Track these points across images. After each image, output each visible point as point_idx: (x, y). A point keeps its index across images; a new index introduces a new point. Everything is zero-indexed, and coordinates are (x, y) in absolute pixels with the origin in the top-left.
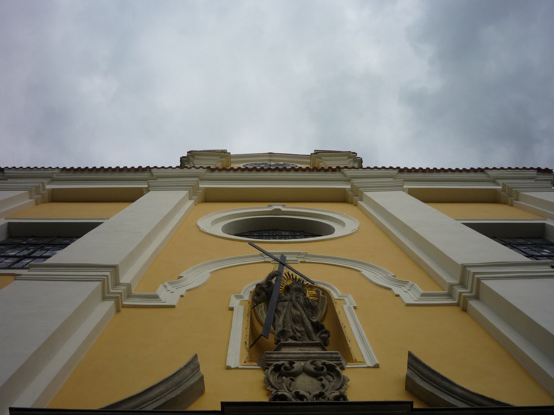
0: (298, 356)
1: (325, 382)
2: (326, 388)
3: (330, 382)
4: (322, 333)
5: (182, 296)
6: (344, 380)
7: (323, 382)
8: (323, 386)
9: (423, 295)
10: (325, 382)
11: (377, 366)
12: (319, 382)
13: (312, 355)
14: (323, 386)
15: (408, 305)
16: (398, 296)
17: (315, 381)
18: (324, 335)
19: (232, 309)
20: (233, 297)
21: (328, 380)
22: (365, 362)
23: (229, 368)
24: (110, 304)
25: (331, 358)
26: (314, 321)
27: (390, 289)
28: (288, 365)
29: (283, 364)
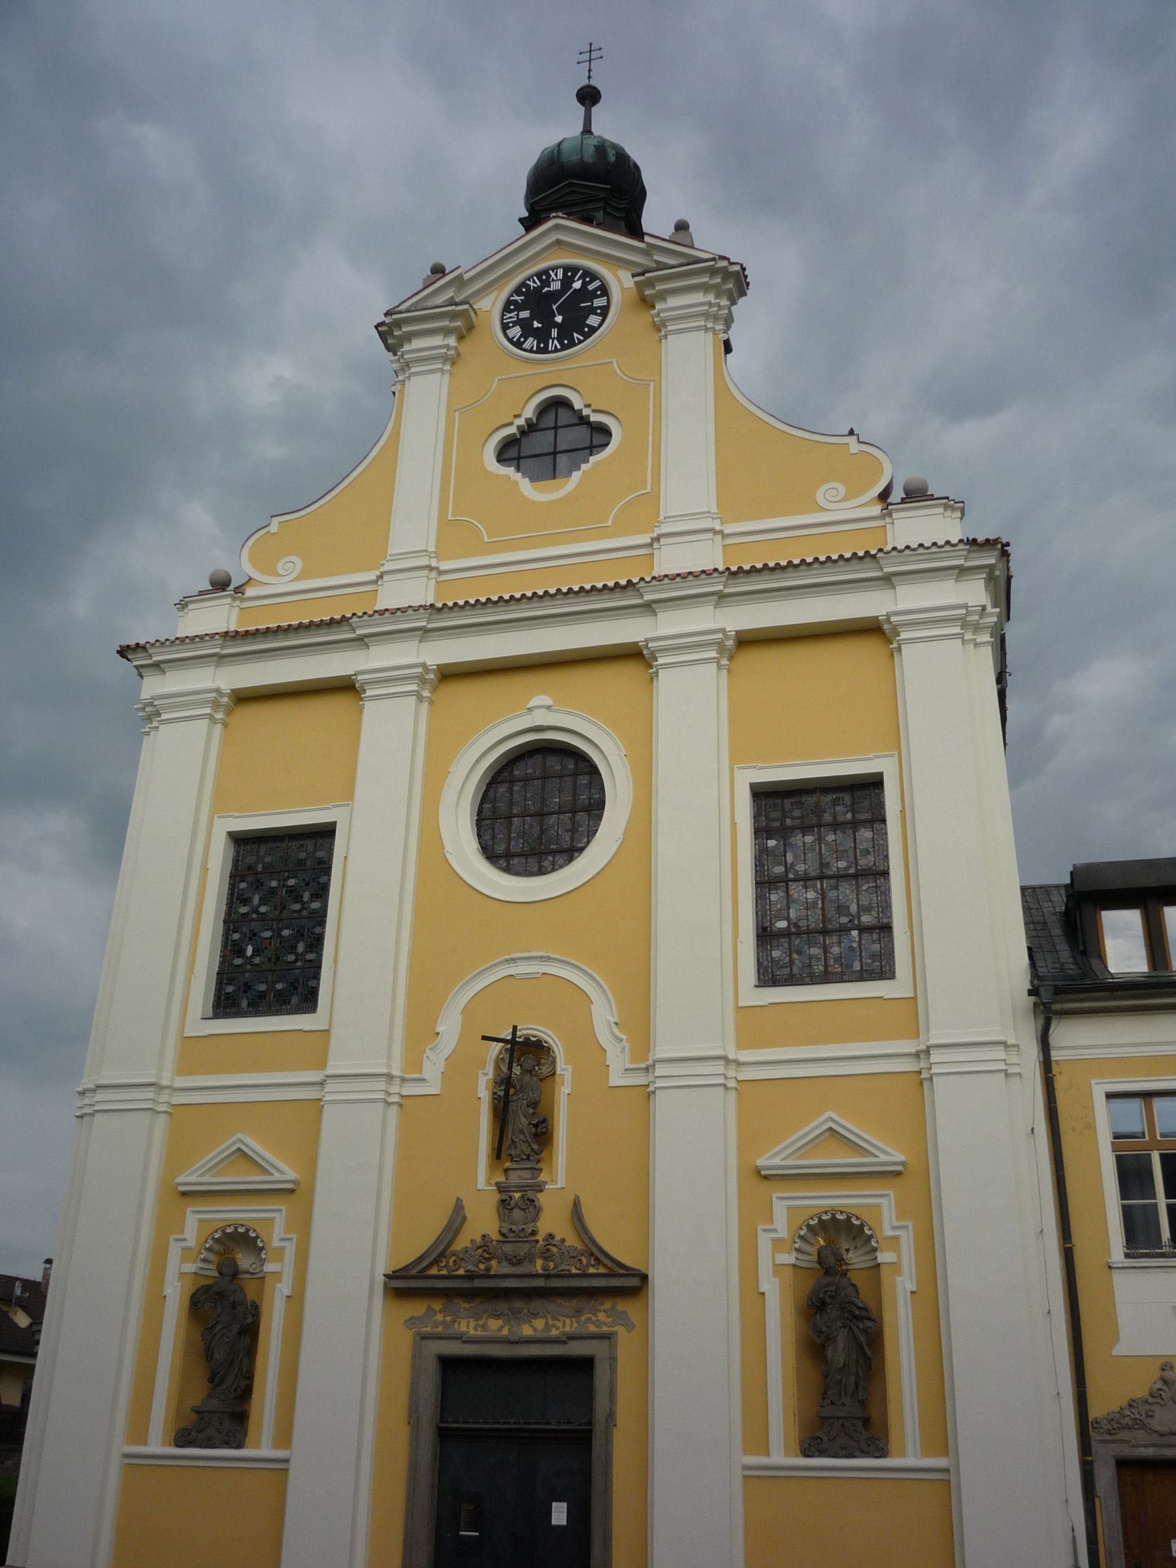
24: (395, 1108)
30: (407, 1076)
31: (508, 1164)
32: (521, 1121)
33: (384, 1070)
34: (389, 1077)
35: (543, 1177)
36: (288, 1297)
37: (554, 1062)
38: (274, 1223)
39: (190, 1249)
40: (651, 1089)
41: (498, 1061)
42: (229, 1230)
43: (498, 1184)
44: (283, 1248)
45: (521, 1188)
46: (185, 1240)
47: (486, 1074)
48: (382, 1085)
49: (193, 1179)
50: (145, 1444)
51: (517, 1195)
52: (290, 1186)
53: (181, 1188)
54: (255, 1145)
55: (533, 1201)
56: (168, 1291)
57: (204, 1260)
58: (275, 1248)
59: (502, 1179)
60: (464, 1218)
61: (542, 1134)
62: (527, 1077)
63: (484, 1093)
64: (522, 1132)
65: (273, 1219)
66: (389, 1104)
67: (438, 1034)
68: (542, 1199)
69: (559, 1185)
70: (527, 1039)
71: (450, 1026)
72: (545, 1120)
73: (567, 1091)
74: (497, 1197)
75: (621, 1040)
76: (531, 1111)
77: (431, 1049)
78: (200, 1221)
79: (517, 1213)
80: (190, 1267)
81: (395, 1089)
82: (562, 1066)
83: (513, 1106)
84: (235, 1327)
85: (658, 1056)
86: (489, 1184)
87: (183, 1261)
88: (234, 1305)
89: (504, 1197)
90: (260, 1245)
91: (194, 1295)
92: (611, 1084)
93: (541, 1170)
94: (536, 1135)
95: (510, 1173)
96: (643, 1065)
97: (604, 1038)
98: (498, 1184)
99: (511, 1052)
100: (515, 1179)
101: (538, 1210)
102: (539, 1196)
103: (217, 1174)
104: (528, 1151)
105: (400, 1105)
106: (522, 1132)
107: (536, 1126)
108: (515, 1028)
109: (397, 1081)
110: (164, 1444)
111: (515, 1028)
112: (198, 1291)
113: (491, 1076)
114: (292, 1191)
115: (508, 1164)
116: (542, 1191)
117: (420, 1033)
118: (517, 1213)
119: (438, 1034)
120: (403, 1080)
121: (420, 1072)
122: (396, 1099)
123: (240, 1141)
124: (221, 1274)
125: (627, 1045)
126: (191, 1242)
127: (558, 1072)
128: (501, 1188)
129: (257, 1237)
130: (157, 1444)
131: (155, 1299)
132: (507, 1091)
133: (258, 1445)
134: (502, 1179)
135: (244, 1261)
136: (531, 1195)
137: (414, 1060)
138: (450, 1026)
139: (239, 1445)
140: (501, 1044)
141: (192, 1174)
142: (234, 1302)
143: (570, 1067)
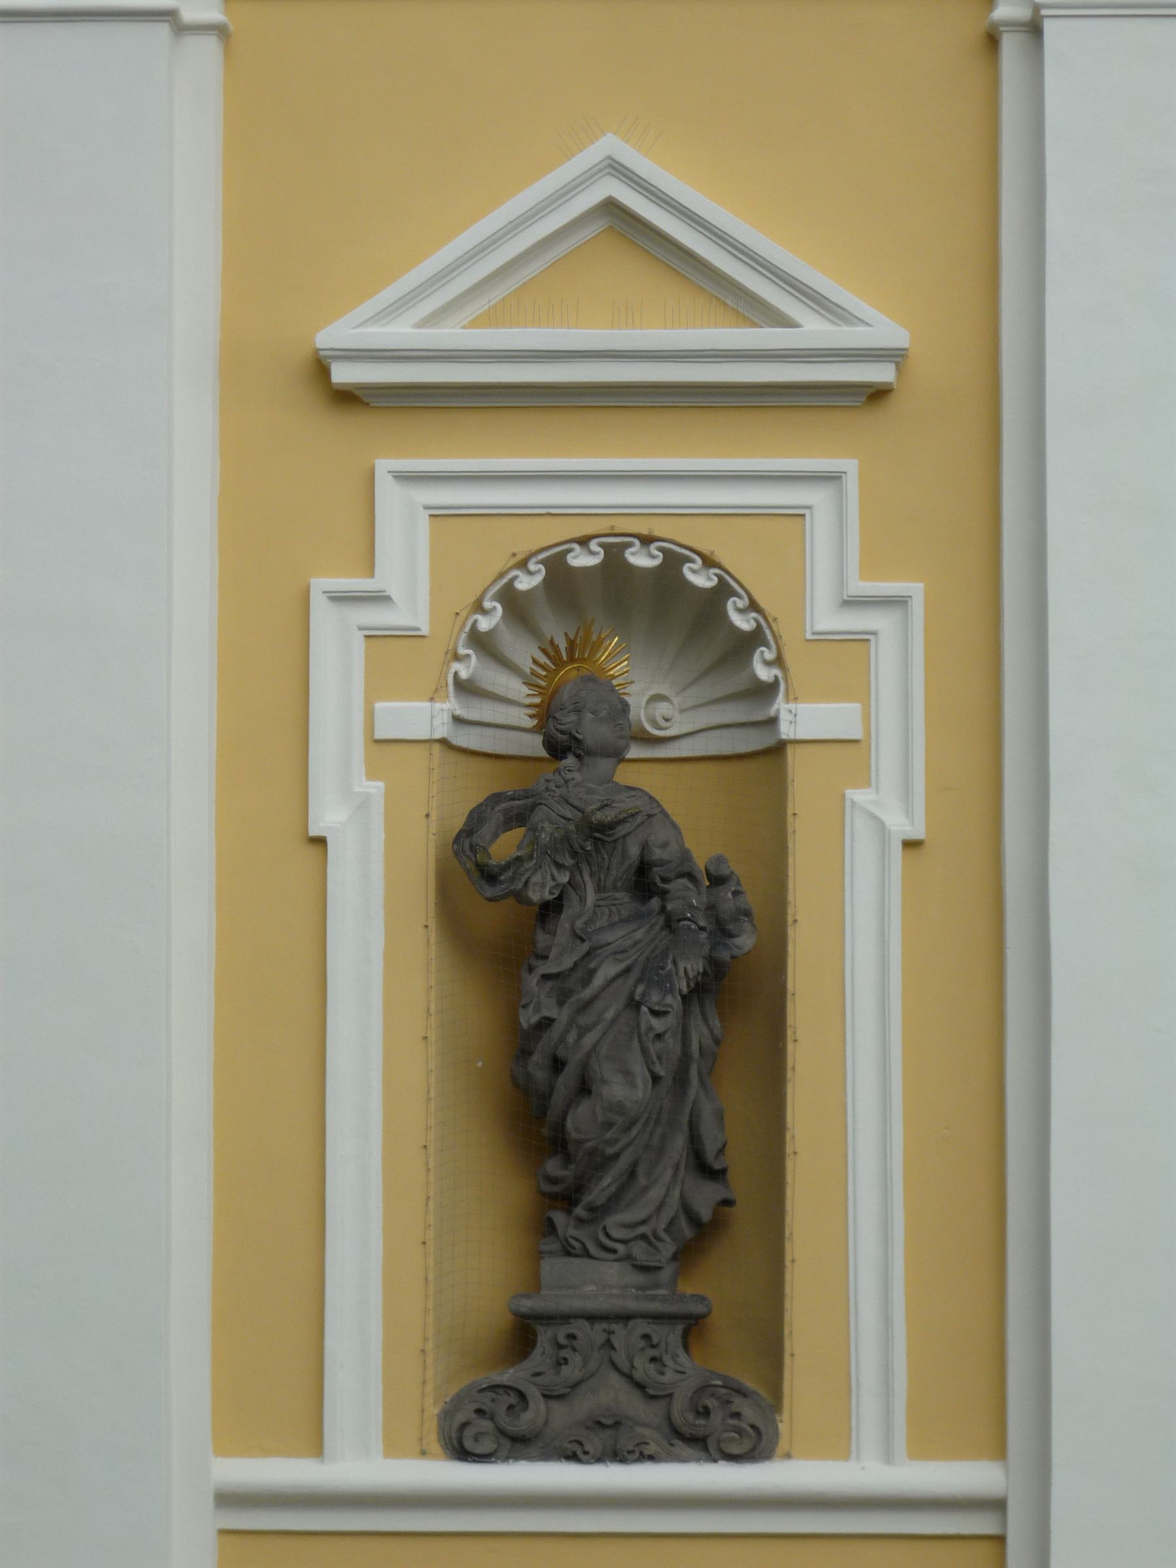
36: (910, 845)
38: (818, 545)
39: (410, 636)
42: (641, 559)
44: (862, 640)
46: (380, 599)
49: (401, 332)
50: (316, 1447)
52: (882, 374)
53: (342, 374)
54: (689, 190)
56: (329, 816)
57: (464, 688)
58: (825, 639)
65: (797, 516)
78: (439, 515)
80: (424, 716)
84: (692, 966)
87: (379, 683)
88: (644, 881)
90: (743, 623)
91: (469, 831)
103: (490, 319)
110: (393, 1449)
112: (476, 819)
114: (877, 394)
123: (615, 168)
124: (557, 749)
126: (411, 609)
129: (723, 591)
130: (369, 1449)
131: (274, 858)
133: (838, 1442)
135: (651, 689)
139: (756, 1446)
141: (375, 319)
142: (643, 868)
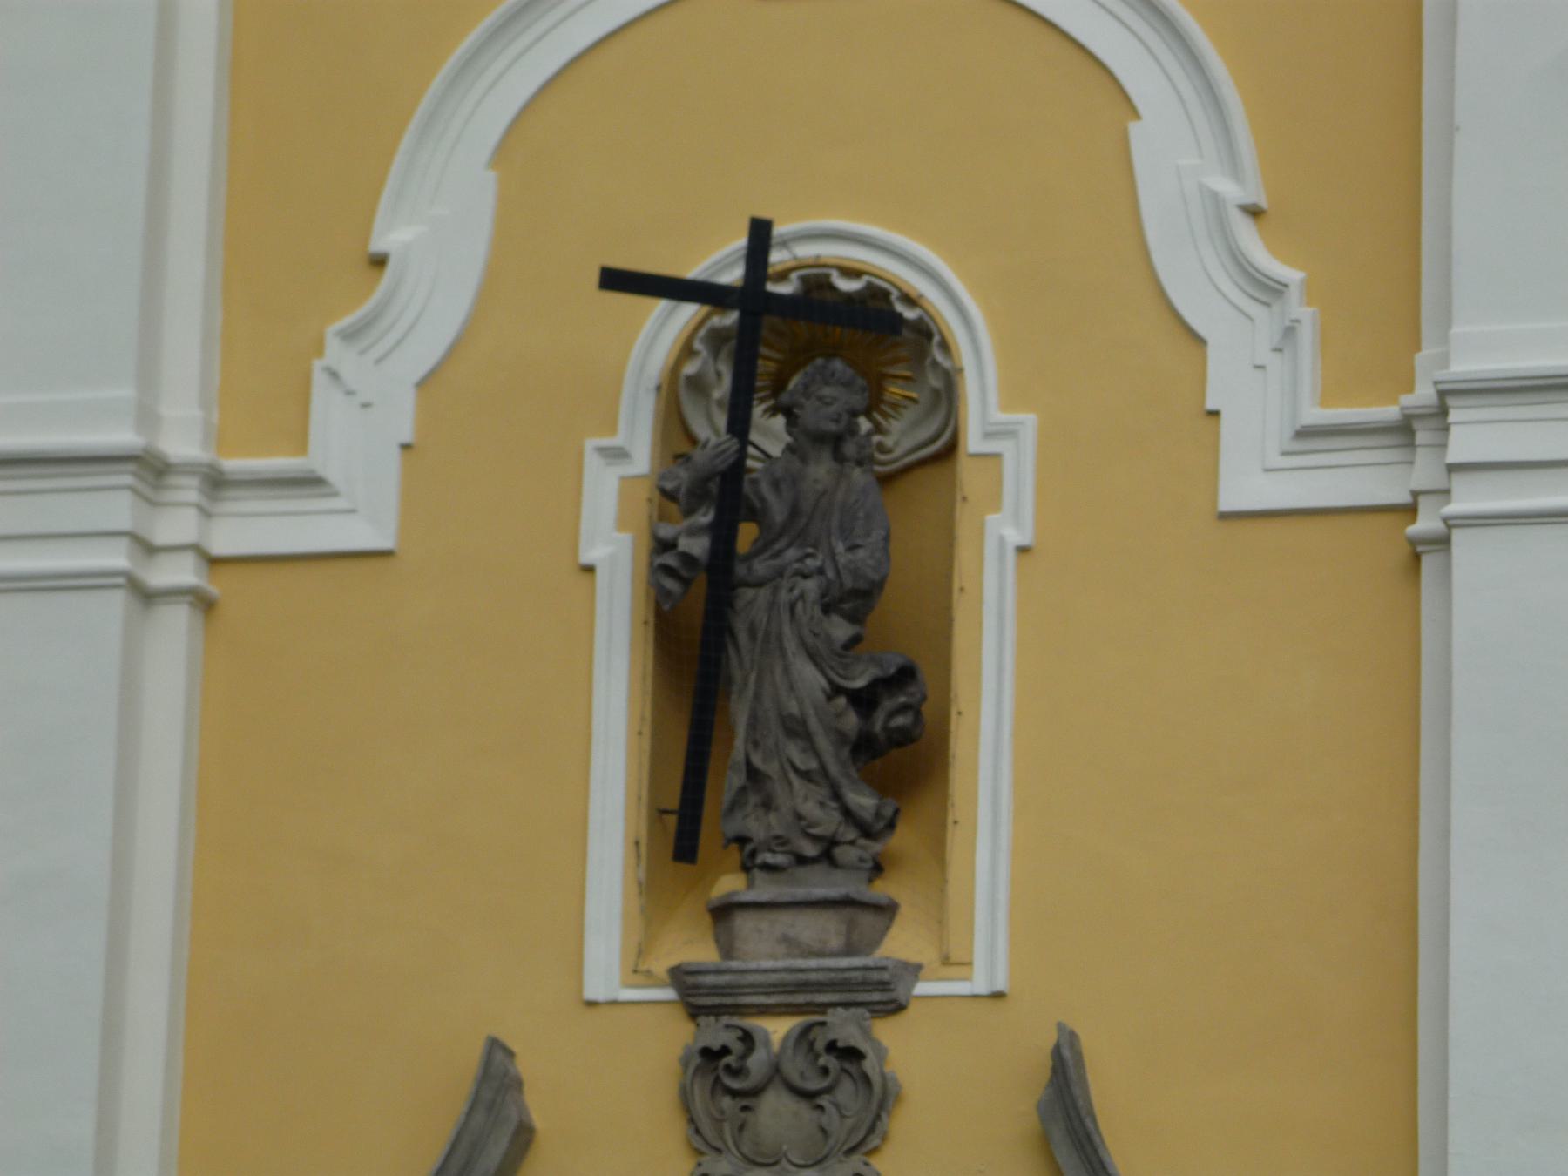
0: (774, 978)
1: (831, 1119)
2: (831, 1141)
3: (843, 1116)
4: (892, 714)
5: (406, 447)
6: (885, 1092)
7: (824, 1120)
8: (823, 1131)
9: (1304, 433)
10: (831, 1119)
11: (998, 996)
12: (816, 1114)
13: (813, 976)
14: (823, 1131)
15: (1225, 516)
16: (1215, 414)
17: (803, 1109)
18: (900, 721)
19: (589, 569)
20: (592, 462)
21: (837, 1105)
22: (970, 964)
23: (591, 1004)
25: (864, 983)
26: (860, 683)
27: (1200, 341)
28: (737, 1047)
29: (725, 1051)
30: (234, 464)
31: (730, 884)
32: (794, 680)
33: (122, 437)
34: (151, 469)
35: (901, 943)
37: (947, 396)
40: (1426, 523)
41: (677, 393)
43: (681, 977)
45: (793, 994)
47: (617, 454)
48: (115, 506)
51: (778, 1029)
55: (853, 1054)
59: (702, 952)
60: (524, 1135)
61: (895, 739)
62: (820, 470)
63: (612, 546)
64: (796, 729)
66: (147, 596)
67: (379, 262)
68: (900, 1046)
69: (980, 985)
70: (816, 284)
71: (438, 224)
72: (906, 674)
73: (1014, 537)
74: (677, 1036)
75: (1270, 290)
76: (841, 630)
77: (350, 335)
79: (777, 1114)
81: (177, 526)
82: (984, 411)
83: (752, 604)
85: (1465, 366)
86: (637, 972)
89: (717, 1034)
92: (1227, 503)
93: (887, 910)
94: (864, 748)
95: (744, 923)
96: (1389, 412)
97: (1197, 285)
98: (681, 977)
99: (743, 350)
100: (763, 949)
101: (880, 1099)
102: (886, 1031)
104: (829, 822)
105: (204, 604)
106: (796, 729)
107: (864, 701)
108: (760, 233)
109: (189, 490)
111: (760, 233)
113: (642, 460)
115: (730, 884)
116: (896, 1008)
117: (295, 252)
118: (777, 1114)
119: (379, 262)
120: (216, 483)
121: (300, 445)
122: (181, 573)
125: (1304, 313)
127: (973, 441)
128: (696, 995)
132: (723, 534)
134: (702, 952)
136: (843, 1027)
137: (268, 385)
138: (438, 224)
140: (689, 311)
143: (1028, 420)
